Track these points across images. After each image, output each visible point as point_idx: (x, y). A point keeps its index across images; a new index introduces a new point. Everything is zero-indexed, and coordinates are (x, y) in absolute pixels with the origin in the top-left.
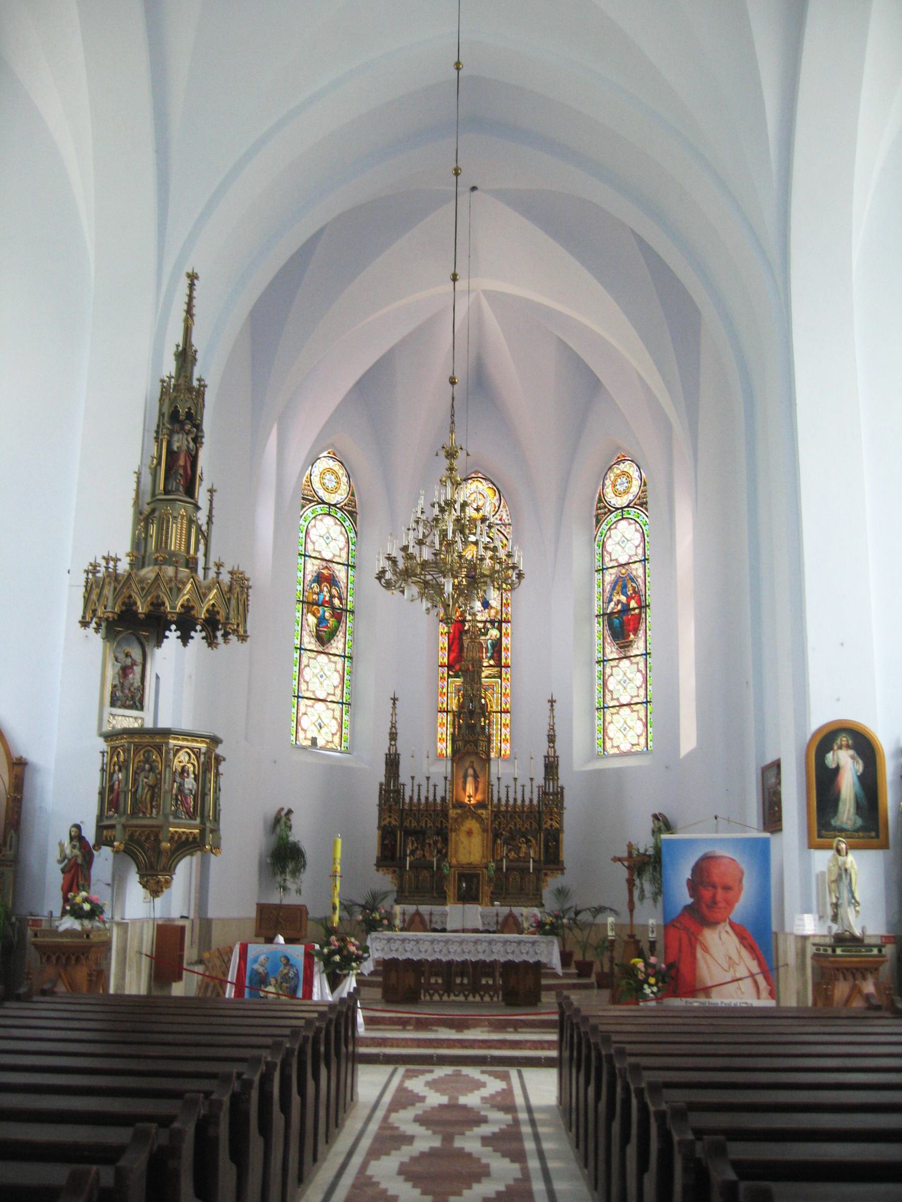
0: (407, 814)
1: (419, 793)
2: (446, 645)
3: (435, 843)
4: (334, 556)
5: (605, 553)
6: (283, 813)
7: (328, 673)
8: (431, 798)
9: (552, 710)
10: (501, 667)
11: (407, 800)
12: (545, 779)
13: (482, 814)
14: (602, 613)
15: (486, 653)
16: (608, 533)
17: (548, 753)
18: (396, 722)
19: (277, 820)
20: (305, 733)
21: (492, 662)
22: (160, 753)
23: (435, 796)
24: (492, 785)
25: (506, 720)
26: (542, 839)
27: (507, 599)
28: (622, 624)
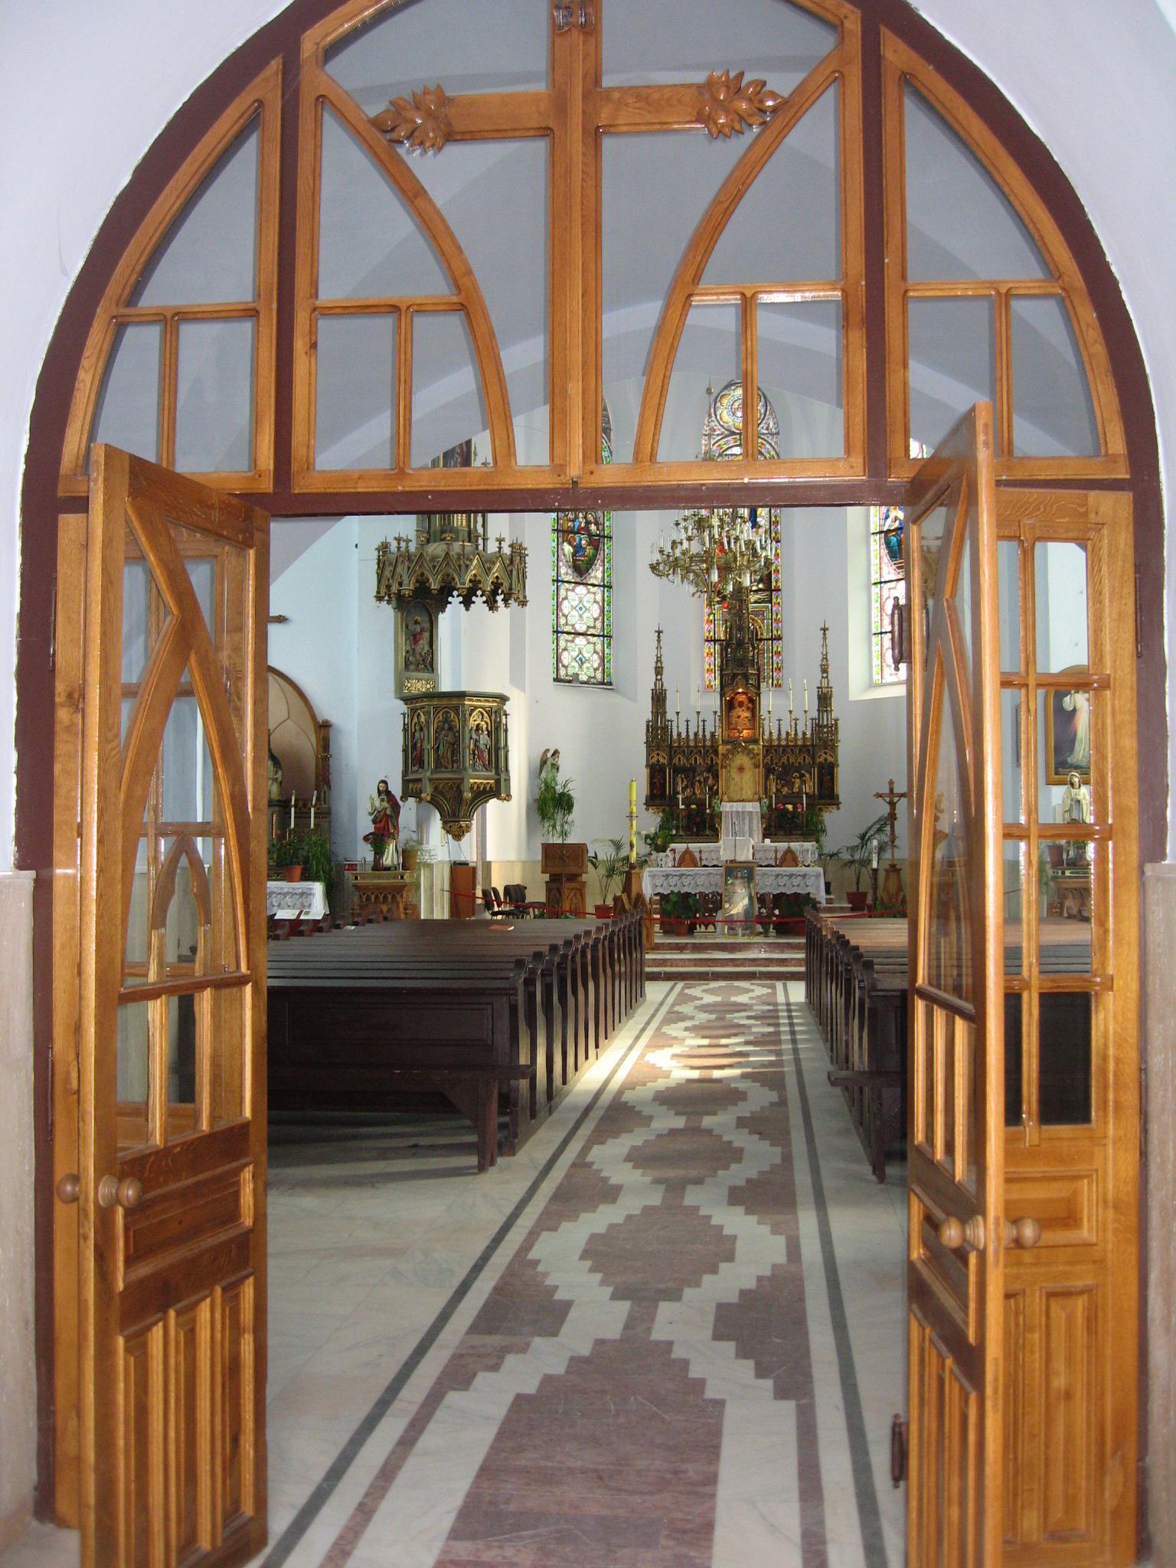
3: (706, 779)
6: (549, 755)
7: (587, 605)
9: (825, 638)
10: (772, 591)
11: (675, 736)
19: (544, 762)
22: (457, 714)
28: (900, 543)
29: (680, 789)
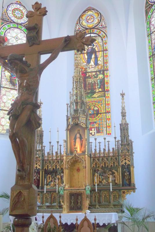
0: (46, 162)
5: (151, 26)
10: (105, 92)
13: (83, 158)
14: (152, 55)
15: (97, 86)
16: (152, 16)
20: (3, 127)
21: (100, 90)
26: (120, 171)
27: (106, 60)
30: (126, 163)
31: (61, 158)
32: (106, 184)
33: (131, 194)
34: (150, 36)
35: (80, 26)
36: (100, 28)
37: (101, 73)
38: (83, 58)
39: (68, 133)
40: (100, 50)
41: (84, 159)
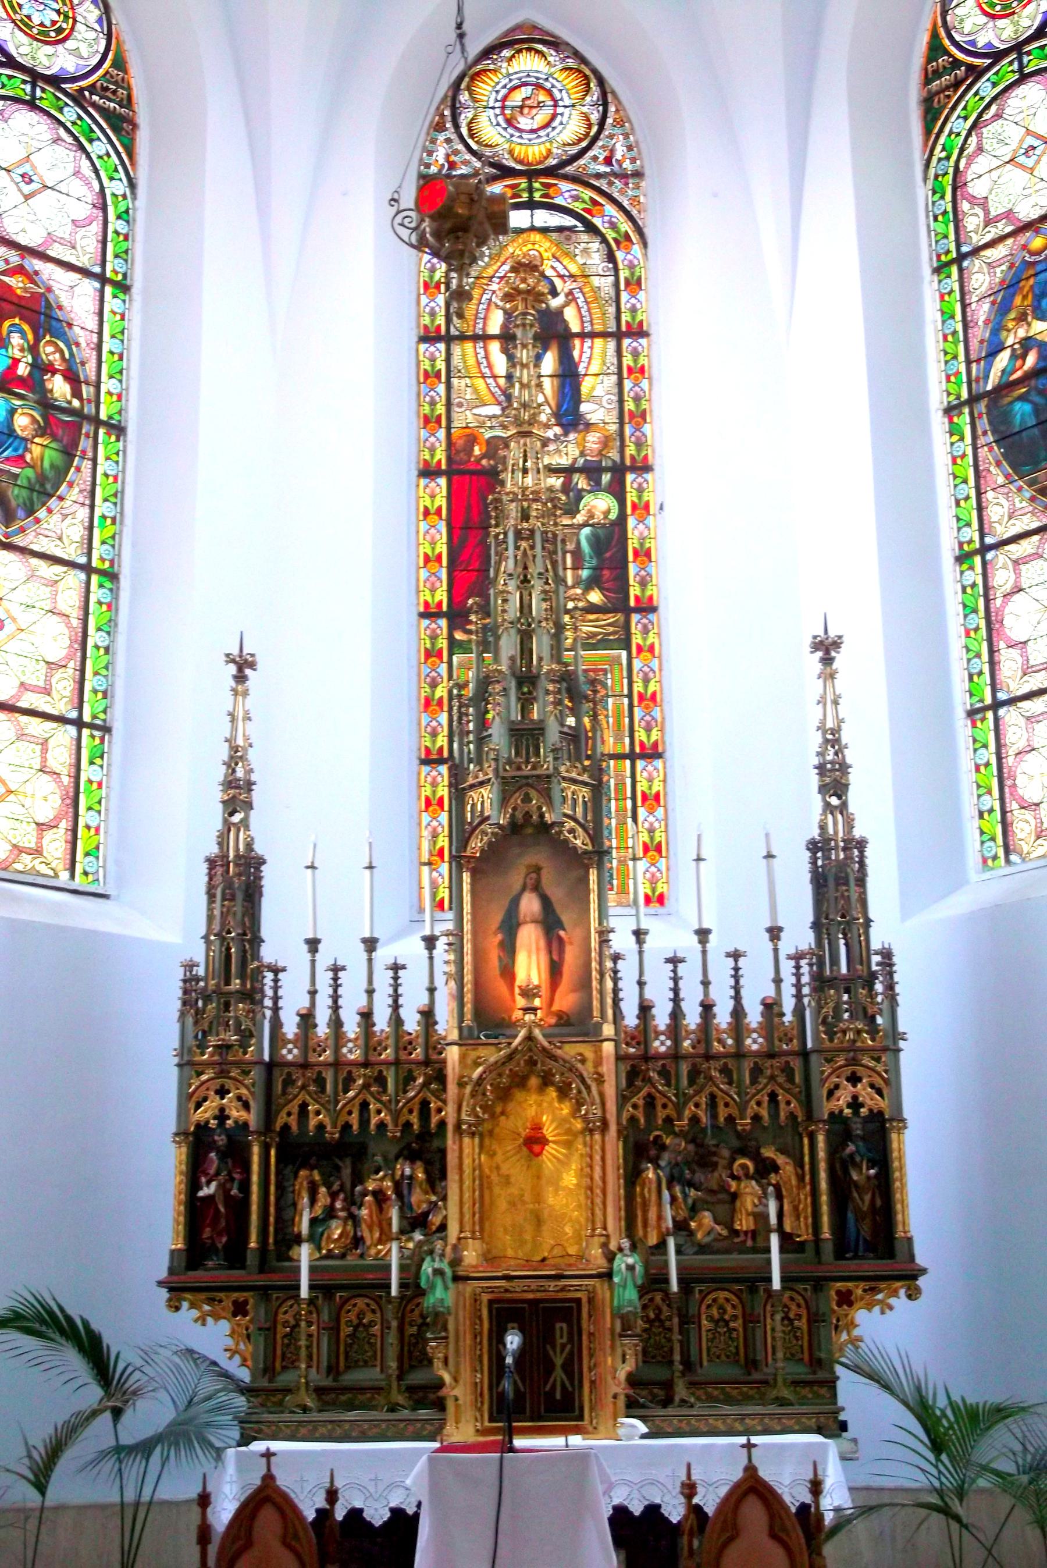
1: (335, 997)
2: (442, 548)
4: (51, 238)
5: (965, 206)
7: (24, 618)
8: (382, 1021)
10: (628, 611)
11: (290, 1027)
12: (816, 926)
13: (583, 1061)
14: (965, 395)
15: (575, 568)
16: (973, 140)
17: (823, 827)
18: (246, 738)
21: (595, 597)
23: (396, 1006)
24: (616, 958)
25: (650, 780)
26: (822, 1154)
27: (637, 399)
29: (305, 1228)
30: (855, 1104)
31: (403, 1056)
32: (719, 1238)
33: (891, 1308)
34: (954, 269)
35: (460, 147)
36: (598, 176)
37: (598, 483)
38: (474, 371)
39: (466, 887)
40: (598, 328)
41: (590, 1065)
